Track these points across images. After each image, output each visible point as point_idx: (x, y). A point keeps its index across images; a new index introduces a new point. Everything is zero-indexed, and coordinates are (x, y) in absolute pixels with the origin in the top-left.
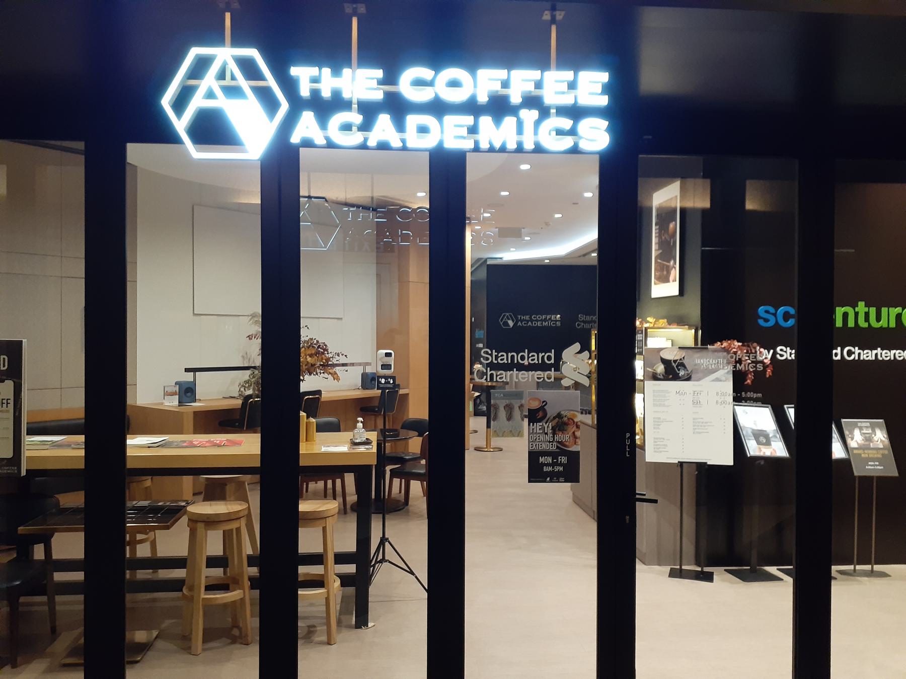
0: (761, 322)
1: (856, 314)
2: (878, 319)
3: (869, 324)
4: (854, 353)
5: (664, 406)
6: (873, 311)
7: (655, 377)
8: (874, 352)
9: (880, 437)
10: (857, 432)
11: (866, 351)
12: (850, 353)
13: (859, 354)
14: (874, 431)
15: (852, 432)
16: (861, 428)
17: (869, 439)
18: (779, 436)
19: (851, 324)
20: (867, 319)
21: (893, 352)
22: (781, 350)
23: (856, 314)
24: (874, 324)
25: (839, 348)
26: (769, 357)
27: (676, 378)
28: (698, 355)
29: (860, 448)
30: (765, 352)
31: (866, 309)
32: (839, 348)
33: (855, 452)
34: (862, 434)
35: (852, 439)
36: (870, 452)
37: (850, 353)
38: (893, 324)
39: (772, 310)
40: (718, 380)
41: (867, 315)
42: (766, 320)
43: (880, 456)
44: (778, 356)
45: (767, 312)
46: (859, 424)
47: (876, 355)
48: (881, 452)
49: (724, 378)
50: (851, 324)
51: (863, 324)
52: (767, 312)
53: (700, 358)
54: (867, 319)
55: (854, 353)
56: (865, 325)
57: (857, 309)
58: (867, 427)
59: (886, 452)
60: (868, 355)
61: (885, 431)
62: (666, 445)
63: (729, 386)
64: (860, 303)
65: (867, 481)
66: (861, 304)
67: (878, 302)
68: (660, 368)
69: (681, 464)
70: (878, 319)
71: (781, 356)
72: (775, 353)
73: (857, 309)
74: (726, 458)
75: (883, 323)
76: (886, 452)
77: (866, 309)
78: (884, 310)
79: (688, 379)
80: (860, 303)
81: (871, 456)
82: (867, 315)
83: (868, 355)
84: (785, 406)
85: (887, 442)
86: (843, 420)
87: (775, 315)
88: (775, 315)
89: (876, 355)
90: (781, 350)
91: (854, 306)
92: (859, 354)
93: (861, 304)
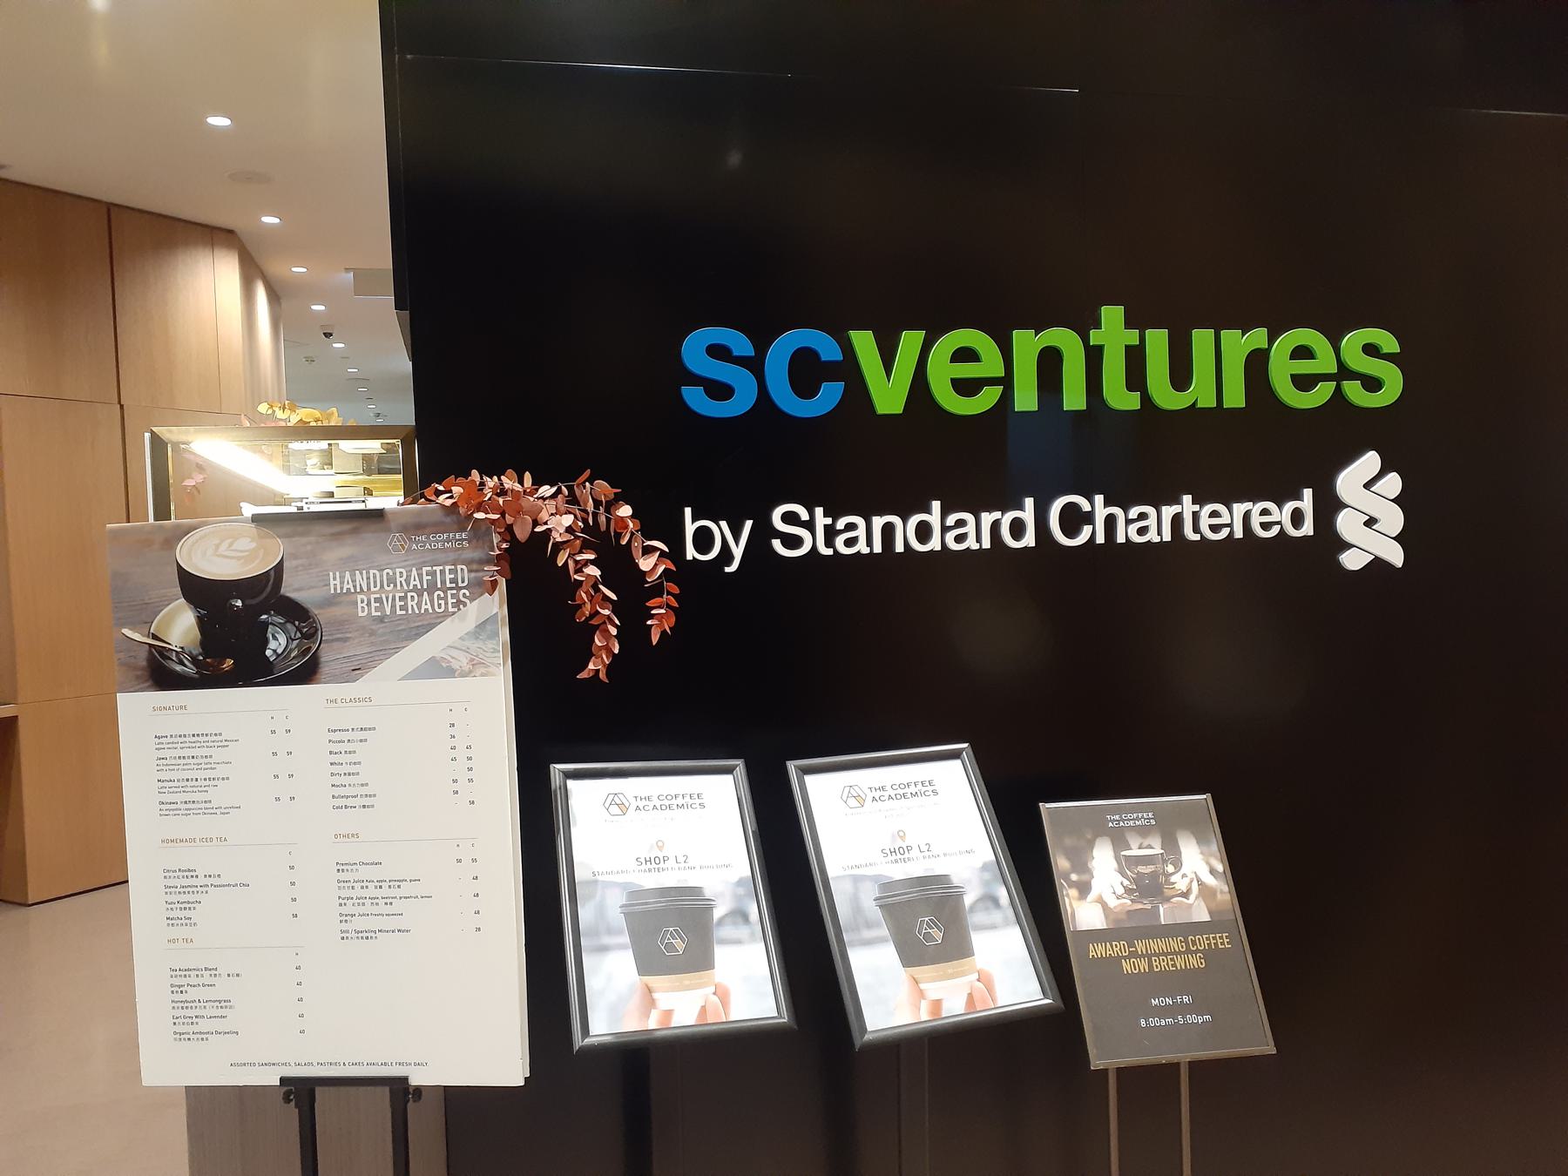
0: (695, 398)
1: (1094, 357)
2: (1181, 376)
3: (1146, 399)
4: (1089, 518)
5: (208, 809)
6: (1157, 342)
7: (162, 673)
8: (1168, 512)
9: (1199, 870)
10: (1103, 859)
11: (1134, 512)
12: (1074, 520)
13: (1110, 521)
14: (1171, 846)
15: (1081, 864)
16: (1119, 841)
17: (1149, 886)
18: (756, 910)
19: (1074, 398)
20: (1136, 376)
21: (1239, 508)
22: (790, 518)
23: (1094, 357)
24: (1167, 398)
25: (1029, 502)
26: (738, 552)
27: (251, 669)
28: (345, 550)
29: (1120, 931)
30: (720, 530)
31: (1133, 337)
32: (1029, 502)
33: (1097, 950)
34: (1126, 864)
35: (1084, 889)
36: (1156, 945)
37: (1074, 520)
38: (1235, 397)
39: (741, 344)
40: (436, 669)
41: (1135, 359)
42: (720, 391)
43: (1195, 962)
44: (777, 544)
45: (718, 352)
46: (1113, 820)
47: (1177, 520)
48: (1203, 941)
49: (462, 661)
50: (1074, 398)
51: (1120, 398)
52: (718, 352)
53: (350, 564)
54: (1136, 376)
55: (1089, 518)
56: (1132, 402)
57: (1095, 337)
58: (1143, 831)
59: (1223, 941)
60: (1147, 525)
61: (1216, 846)
62: (224, 1003)
63: (487, 703)
64: (1106, 311)
65: (1148, 1083)
66: (1112, 315)
67: (1175, 308)
68: (181, 627)
69: (301, 1093)
70: (1181, 376)
71: (792, 542)
72: (764, 532)
73: (1095, 337)
74: (498, 1057)
75: (1200, 392)
76: (1223, 941)
77: (1133, 337)
78: (1202, 339)
79: (306, 673)
80: (1106, 311)
81: (1160, 964)
82: (1135, 359)
83: (1147, 525)
84: (792, 766)
85: (1223, 890)
86: (1045, 807)
87: (755, 365)
88: (755, 365)
89: (1177, 520)
90: (790, 518)
91: (1084, 323)
92: (1110, 521)
93: (1112, 315)
